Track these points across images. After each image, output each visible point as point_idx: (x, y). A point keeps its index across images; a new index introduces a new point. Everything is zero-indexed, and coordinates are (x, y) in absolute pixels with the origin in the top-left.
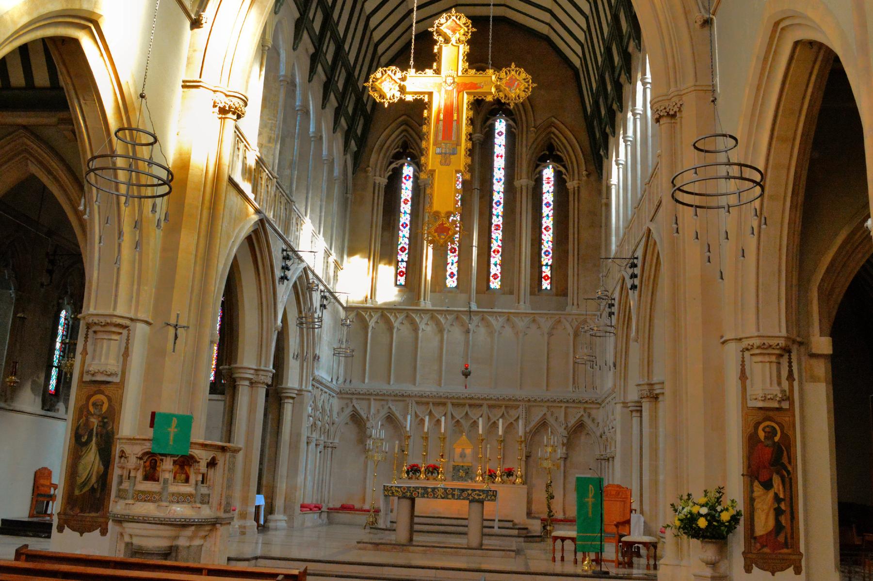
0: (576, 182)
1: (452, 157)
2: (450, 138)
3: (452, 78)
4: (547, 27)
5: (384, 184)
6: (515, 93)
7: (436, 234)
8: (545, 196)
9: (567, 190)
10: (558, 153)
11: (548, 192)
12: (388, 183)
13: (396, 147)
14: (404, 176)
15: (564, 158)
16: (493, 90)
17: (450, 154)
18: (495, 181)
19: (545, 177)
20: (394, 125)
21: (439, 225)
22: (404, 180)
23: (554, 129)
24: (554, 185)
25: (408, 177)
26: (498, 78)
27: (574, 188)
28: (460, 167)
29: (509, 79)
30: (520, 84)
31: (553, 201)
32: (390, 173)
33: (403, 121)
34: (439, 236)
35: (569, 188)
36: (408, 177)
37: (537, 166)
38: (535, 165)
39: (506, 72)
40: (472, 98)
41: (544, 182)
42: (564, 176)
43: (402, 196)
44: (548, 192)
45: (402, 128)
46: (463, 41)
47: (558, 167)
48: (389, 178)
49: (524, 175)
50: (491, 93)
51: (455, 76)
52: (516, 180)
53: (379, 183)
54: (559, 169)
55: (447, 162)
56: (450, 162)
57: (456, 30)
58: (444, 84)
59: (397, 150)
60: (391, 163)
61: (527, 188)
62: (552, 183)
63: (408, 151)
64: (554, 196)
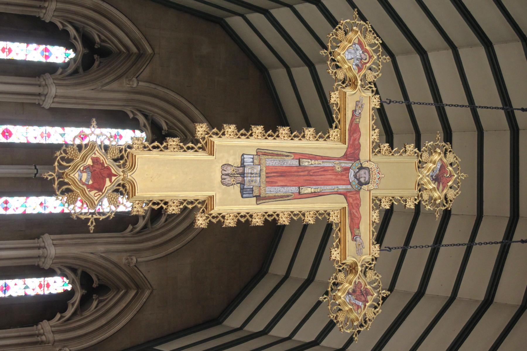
0: (51, 337)
1: (237, 188)
2: (270, 183)
3: (367, 180)
4: (282, 272)
5: (42, 15)
6: (344, 302)
7: (89, 162)
8: (19, 282)
9: (35, 321)
10: (95, 303)
11: (27, 287)
12: (44, 21)
13: (103, 37)
14: (49, 47)
15: (87, 313)
16: (349, 260)
17: (242, 184)
18: (42, 199)
19: (50, 280)
20: (138, 34)
21: (108, 168)
22: (43, 47)
23: (132, 293)
24: (37, 296)
25: (47, 54)
26: (367, 267)
27: (39, 335)
28: (222, 204)
29: (366, 289)
30: (359, 310)
31: (10, 296)
32: (60, 26)
33: (145, 50)
34: (87, 168)
35: (39, 326)
36: (47, 54)
37: (74, 270)
38: (77, 267)
39: (376, 280)
40: (334, 219)
41: (42, 279)
42: (58, 316)
43: (17, 44)
44: (27, 287)
45: (134, 49)
46: (421, 196)
47: (73, 304)
48: (52, 24)
49: (60, 251)
50: (344, 254)
51: (370, 186)
52: (53, 237)
53: (46, 8)
54: (70, 307)
55: (228, 180)
56: (227, 185)
57: (439, 184)
58: (357, 164)
59: (97, 39)
60: (77, 29)
61: (39, 257)
62: (42, 293)
63: (96, 56)
64: (19, 298)
